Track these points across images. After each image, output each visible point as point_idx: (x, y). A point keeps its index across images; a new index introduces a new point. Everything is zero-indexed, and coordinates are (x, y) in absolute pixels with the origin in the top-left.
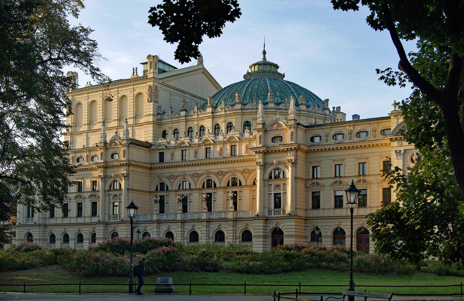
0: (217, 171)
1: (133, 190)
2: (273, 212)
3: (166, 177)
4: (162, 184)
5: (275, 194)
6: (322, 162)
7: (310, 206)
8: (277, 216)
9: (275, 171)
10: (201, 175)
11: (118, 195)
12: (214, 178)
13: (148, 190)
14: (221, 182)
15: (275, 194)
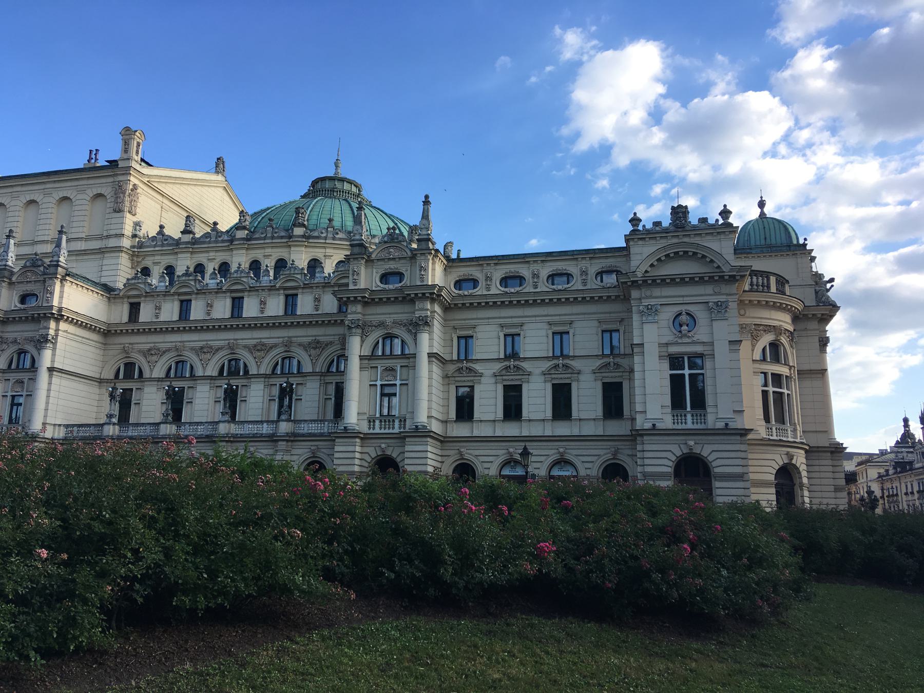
0: (254, 342)
1: (61, 371)
2: (377, 423)
3: (140, 351)
4: (129, 366)
5: (382, 385)
6: (478, 329)
7: (453, 415)
8: (387, 431)
9: (384, 339)
10: (218, 349)
11: (26, 381)
12: (246, 357)
13: (97, 376)
14: (259, 366)
15: (382, 385)
